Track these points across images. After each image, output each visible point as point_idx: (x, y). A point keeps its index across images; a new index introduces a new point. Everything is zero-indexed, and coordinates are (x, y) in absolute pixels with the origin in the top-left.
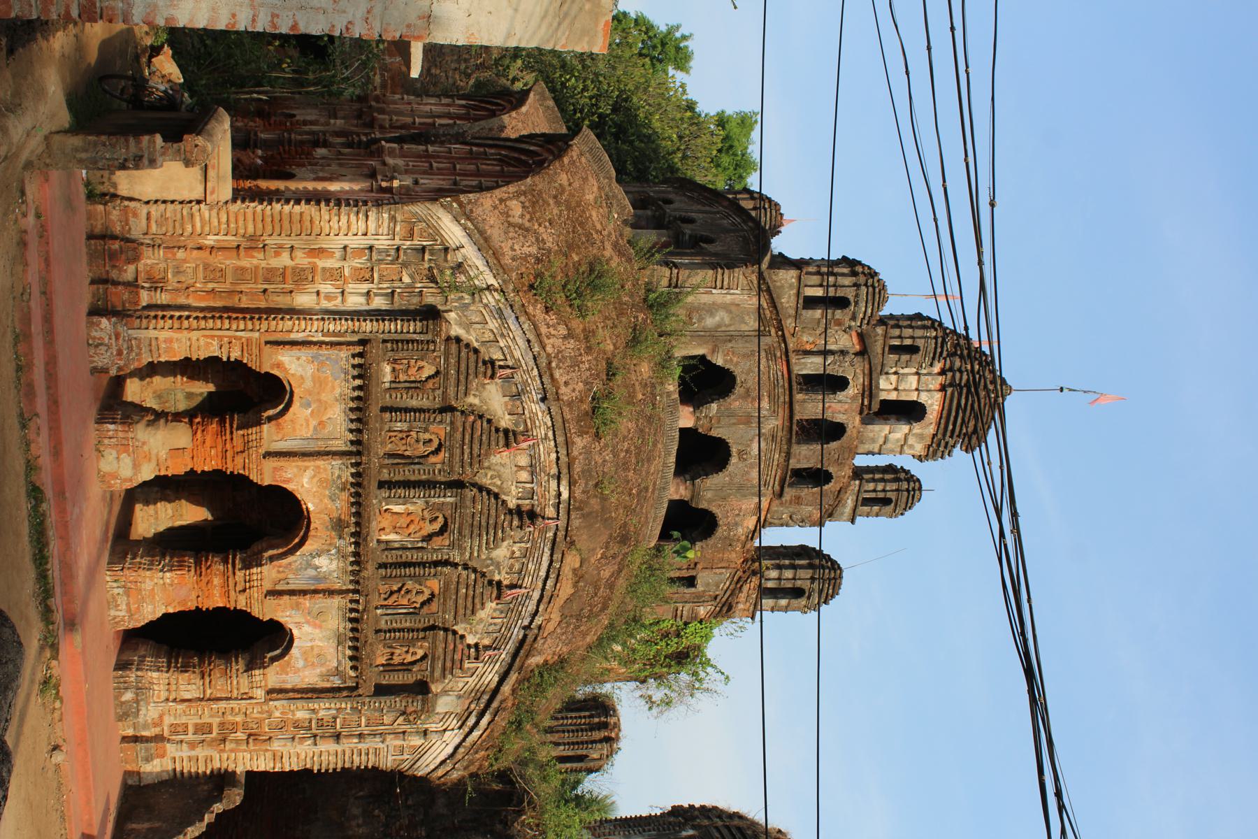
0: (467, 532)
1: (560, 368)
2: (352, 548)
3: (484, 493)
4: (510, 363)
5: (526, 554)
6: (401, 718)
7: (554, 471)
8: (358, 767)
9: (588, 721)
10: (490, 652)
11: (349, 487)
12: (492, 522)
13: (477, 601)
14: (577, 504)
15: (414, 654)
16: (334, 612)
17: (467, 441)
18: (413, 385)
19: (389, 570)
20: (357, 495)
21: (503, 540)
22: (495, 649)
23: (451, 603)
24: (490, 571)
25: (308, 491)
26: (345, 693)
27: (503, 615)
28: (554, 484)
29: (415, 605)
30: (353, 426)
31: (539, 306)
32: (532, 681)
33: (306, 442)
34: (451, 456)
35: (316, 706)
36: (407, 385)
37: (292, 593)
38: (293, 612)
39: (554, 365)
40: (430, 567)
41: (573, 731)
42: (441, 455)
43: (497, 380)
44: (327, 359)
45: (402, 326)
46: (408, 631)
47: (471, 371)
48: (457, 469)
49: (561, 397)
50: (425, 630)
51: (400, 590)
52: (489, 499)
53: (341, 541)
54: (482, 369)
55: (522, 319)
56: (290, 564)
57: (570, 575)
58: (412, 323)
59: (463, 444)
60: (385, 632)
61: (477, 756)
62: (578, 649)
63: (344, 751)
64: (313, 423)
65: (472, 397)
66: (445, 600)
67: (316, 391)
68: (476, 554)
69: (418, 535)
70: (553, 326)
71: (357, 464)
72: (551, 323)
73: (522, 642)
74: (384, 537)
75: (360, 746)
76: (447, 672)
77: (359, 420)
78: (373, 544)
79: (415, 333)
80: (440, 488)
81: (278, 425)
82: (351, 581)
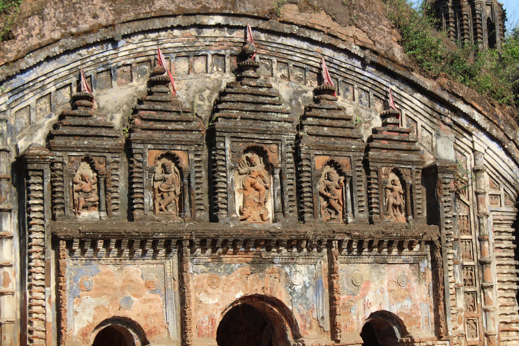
0: (262, 126)
1: (78, 23)
2: (284, 251)
3: (220, 106)
4: (74, 80)
5: (284, 63)
6: (462, 197)
7: (193, 32)
8: (514, 242)
9: (451, 20)
10: (391, 102)
11: (217, 254)
12: (250, 99)
13: (336, 115)
14: (229, 6)
15: (393, 182)
16: (352, 268)
17: (162, 126)
18: (102, 186)
19: (306, 210)
20: (225, 243)
21: (270, 87)
22: (387, 97)
23: (340, 143)
24: (304, 101)
25: (223, 298)
26: (438, 255)
27: (350, 88)
28: (207, 32)
29: (342, 181)
30: (150, 252)
31: (7, 46)
32: (419, 57)
33: (169, 302)
34: (179, 142)
35: (452, 286)
36: (102, 192)
37: (333, 313)
38: (353, 311)
39: (74, 30)
40: (302, 166)
41: (463, 35)
42: (179, 153)
43: (94, 93)
44: (75, 281)
45: (36, 198)
46: (370, 189)
47: (84, 122)
48: (194, 136)
49: (110, 22)
50: (368, 172)
51: (326, 198)
52: (226, 102)
54: (81, 111)
55: (23, 65)
56: (302, 316)
57: (306, 15)
58: (32, 187)
60: (371, 214)
61: (501, 115)
62: (384, 9)
63: (497, 257)
64: (147, 294)
65: (114, 121)
66: (336, 149)
67: (112, 292)
68: (286, 116)
69: (266, 178)
70: (29, 31)
71: (192, 244)
72: (27, 33)
73: (380, 68)
74: (271, 216)
75: (492, 240)
76: (413, 147)
77: (143, 245)
78: (278, 226)
79: (42, 184)
80: (214, 155)
81: (151, 333)
82: (319, 251)
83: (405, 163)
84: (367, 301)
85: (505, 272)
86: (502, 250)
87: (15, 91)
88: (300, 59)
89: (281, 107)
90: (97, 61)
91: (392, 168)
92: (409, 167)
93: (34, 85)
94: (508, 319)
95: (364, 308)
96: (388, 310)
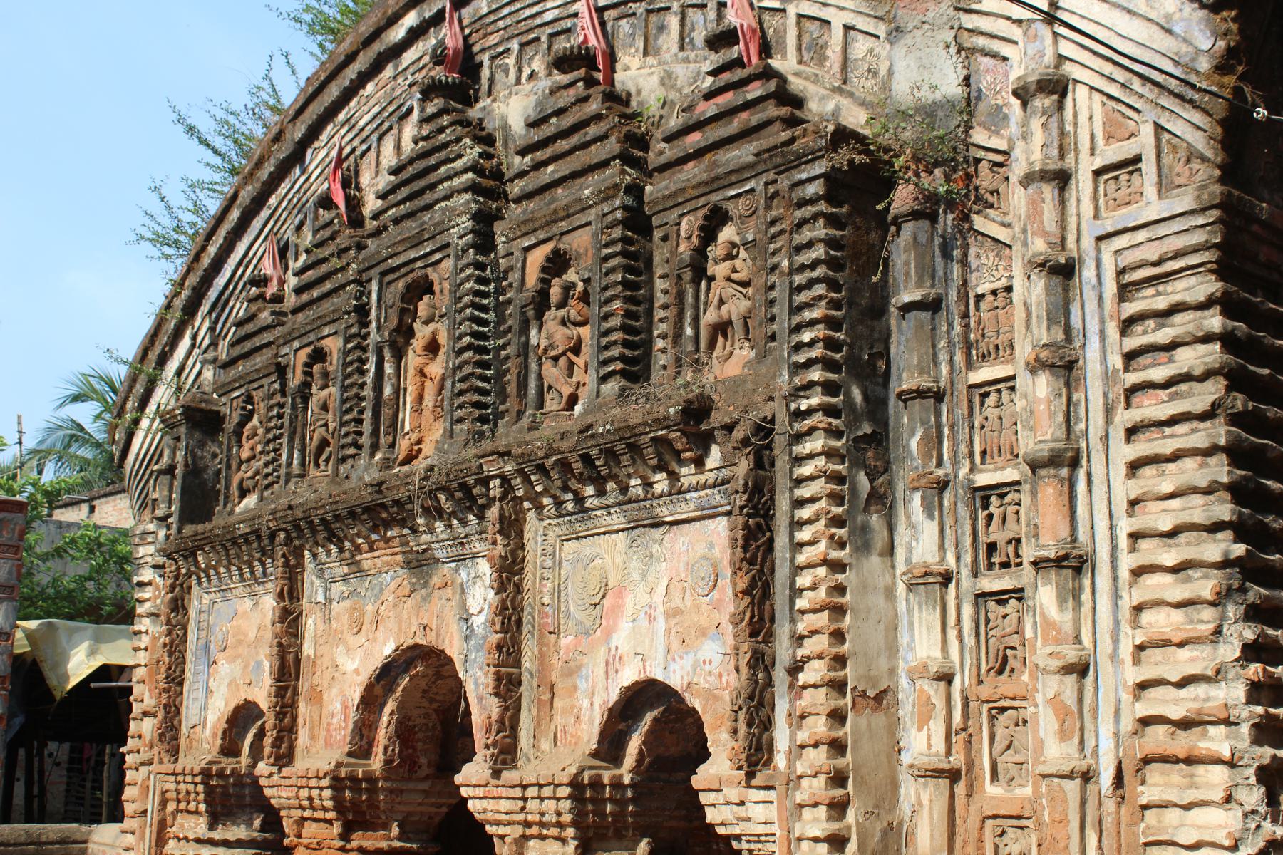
6: (979, 222)
7: (389, 71)
11: (347, 554)
16: (586, 548)
25: (365, 659)
38: (582, 685)
53: (440, 553)
55: (206, 261)
56: (480, 699)
59: (312, 302)
83: (733, 178)
84: (613, 652)
85: (1167, 488)
86: (1163, 394)
87: (220, 304)
88: (556, 12)
89: (464, 159)
90: (291, 206)
91: (705, 211)
92: (747, 187)
93: (235, 288)
94: (1174, 704)
95: (607, 673)
96: (660, 678)
